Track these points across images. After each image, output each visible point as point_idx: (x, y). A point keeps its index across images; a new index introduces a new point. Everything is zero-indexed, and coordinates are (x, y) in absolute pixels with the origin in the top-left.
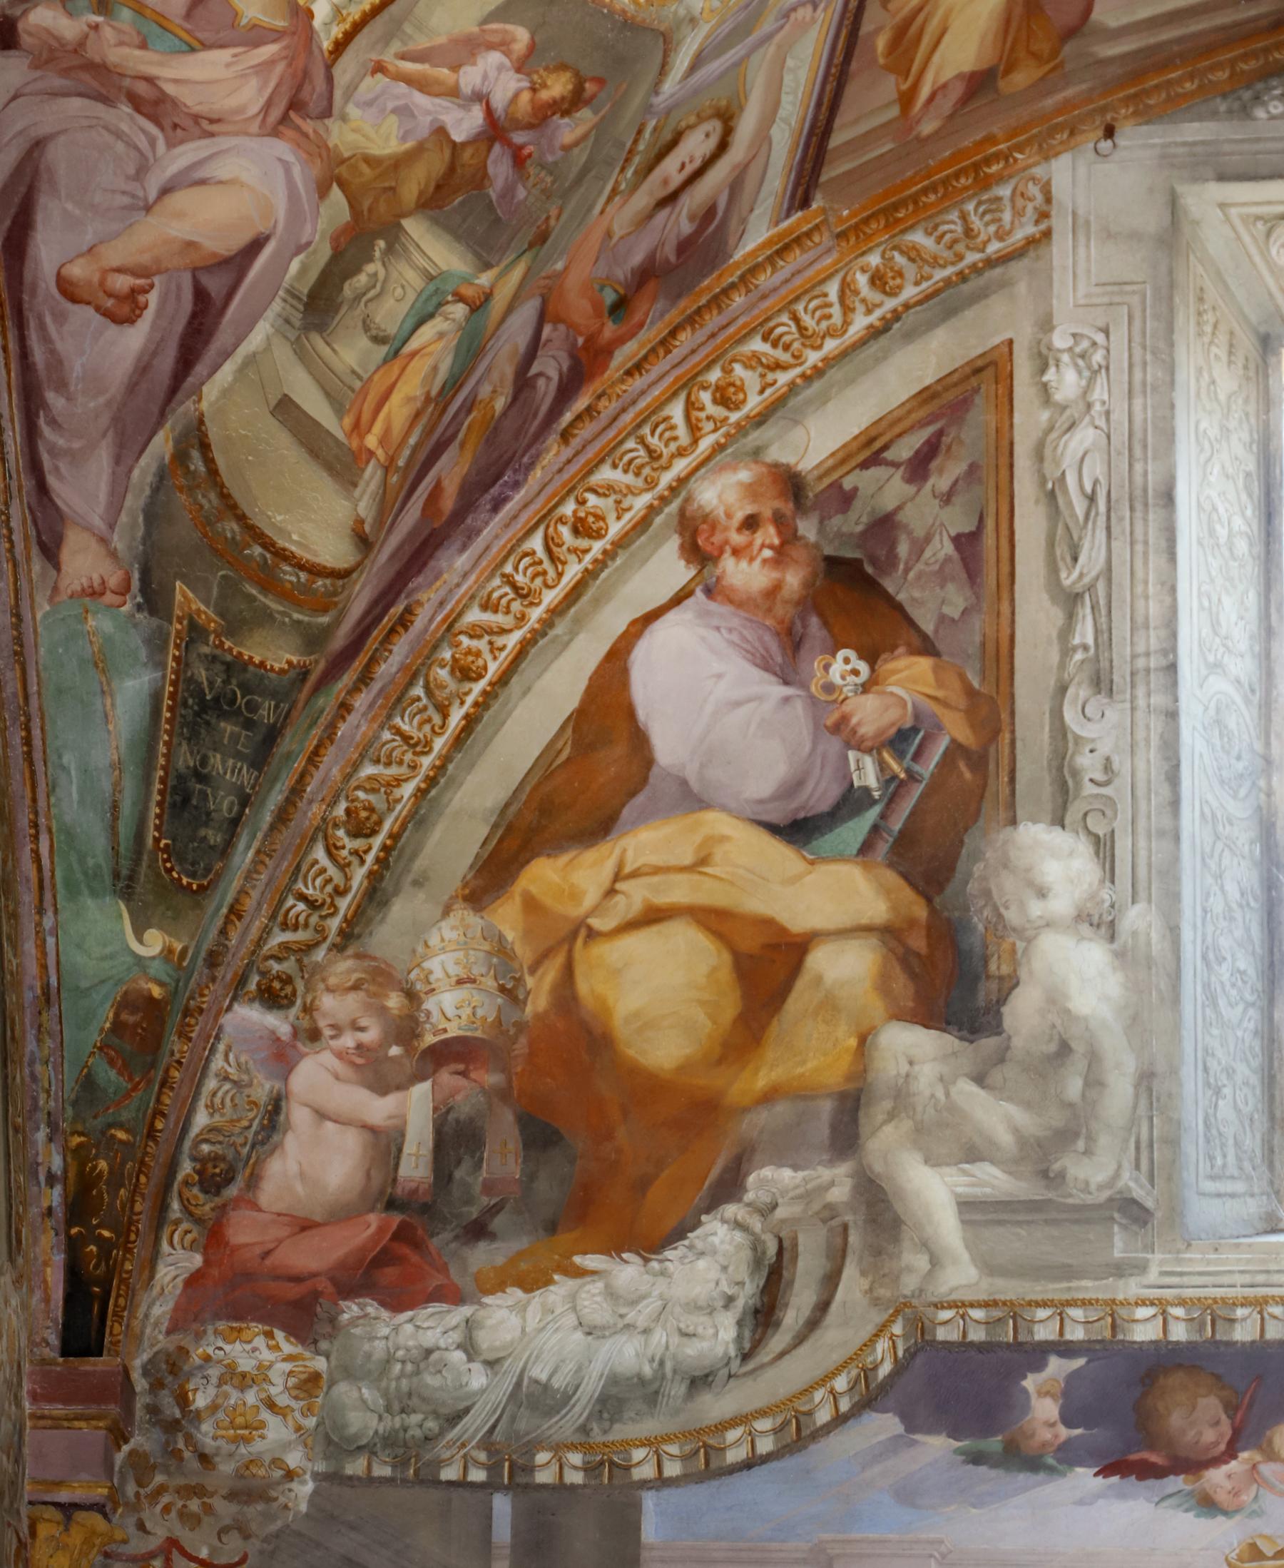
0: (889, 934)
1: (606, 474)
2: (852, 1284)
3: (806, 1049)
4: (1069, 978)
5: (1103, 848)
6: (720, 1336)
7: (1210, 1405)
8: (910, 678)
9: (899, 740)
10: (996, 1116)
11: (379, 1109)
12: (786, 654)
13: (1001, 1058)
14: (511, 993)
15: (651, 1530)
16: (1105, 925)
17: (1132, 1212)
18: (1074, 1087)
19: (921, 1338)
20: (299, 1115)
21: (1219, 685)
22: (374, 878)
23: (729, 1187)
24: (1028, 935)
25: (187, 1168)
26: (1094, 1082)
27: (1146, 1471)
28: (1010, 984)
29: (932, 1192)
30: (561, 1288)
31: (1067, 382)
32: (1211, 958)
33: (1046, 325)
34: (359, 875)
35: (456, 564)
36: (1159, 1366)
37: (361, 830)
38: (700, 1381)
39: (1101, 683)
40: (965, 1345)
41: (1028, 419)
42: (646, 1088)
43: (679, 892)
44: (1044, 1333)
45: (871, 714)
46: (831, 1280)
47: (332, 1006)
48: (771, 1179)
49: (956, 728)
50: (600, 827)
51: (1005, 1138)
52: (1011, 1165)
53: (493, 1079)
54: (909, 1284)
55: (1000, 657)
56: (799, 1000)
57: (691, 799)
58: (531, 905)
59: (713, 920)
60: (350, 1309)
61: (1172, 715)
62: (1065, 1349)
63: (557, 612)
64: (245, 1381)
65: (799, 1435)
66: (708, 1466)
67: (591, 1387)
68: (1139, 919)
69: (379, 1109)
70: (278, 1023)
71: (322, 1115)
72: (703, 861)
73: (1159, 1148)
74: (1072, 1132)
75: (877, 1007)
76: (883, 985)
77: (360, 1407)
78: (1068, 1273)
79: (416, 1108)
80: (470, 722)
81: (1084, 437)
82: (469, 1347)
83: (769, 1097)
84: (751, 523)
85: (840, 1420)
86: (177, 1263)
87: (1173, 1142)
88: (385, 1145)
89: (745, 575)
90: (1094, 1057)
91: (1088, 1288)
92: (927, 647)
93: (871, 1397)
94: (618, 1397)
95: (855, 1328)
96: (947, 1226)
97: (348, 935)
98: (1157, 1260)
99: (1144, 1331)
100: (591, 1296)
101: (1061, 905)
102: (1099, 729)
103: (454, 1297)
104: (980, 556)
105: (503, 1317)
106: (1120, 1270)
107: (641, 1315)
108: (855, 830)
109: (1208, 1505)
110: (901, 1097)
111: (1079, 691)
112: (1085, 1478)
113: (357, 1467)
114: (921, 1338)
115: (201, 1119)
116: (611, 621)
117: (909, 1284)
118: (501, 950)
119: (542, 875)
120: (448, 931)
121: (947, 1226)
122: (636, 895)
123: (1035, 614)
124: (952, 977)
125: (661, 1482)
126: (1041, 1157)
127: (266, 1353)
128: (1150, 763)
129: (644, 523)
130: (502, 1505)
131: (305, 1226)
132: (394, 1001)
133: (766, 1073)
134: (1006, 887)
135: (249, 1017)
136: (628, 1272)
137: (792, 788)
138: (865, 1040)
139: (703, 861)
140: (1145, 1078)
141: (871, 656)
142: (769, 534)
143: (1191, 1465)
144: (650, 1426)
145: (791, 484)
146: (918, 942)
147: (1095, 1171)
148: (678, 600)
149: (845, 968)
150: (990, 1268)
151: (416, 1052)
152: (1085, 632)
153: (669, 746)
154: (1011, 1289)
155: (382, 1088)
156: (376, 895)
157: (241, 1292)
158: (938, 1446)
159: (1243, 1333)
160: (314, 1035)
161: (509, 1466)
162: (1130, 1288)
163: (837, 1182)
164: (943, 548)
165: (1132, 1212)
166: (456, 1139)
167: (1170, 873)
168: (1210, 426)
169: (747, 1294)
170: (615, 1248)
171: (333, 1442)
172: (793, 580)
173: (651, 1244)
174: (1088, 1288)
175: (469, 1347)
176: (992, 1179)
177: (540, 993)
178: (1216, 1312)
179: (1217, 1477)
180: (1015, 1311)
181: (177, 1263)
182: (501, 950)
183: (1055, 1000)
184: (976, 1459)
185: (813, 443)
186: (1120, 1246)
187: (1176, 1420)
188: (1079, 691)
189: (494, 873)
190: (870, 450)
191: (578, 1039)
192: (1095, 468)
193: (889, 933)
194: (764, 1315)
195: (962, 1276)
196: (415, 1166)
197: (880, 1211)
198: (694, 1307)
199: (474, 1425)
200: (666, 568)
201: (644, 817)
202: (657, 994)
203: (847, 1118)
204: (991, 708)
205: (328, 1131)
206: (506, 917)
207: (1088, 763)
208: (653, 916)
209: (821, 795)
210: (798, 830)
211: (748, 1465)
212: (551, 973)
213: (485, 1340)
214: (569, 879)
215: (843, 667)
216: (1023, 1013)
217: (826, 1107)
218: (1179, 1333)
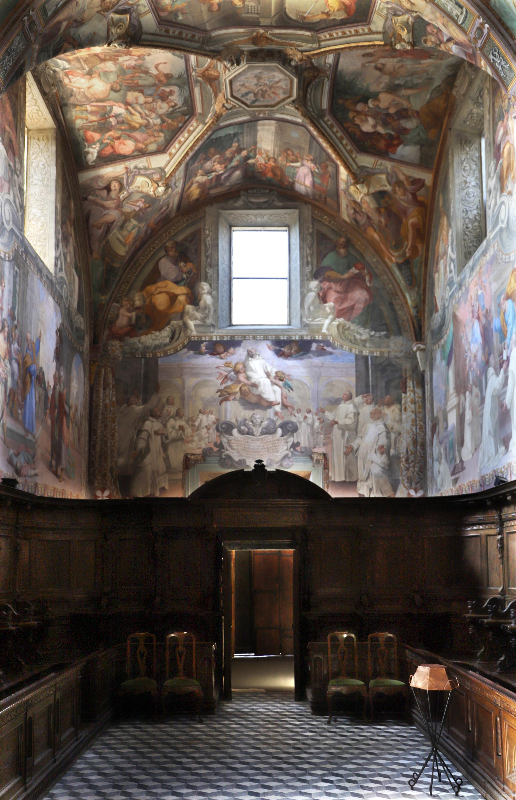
0: (187, 295)
1: (156, 242)
2: (182, 334)
3: (177, 307)
4: (207, 299)
5: (210, 285)
6: (168, 340)
7: (222, 347)
8: (190, 265)
9: (188, 272)
10: (198, 315)
11: (129, 315)
12: (176, 262)
13: (199, 308)
14: (145, 301)
15: (159, 362)
16: (210, 293)
17: (213, 326)
18: (207, 312)
19: (190, 341)
20: (120, 316)
21: (224, 266)
22: (130, 288)
23: (169, 323)
24: (202, 294)
25: (108, 322)
26: (209, 311)
27: (215, 355)
28: (200, 300)
29: (191, 324)
30: (149, 336)
31: (207, 232)
32: (222, 296)
33: (205, 226)
34: (127, 288)
35: (140, 253)
36: (216, 342)
37: (128, 282)
38: (165, 345)
39: (210, 266)
40: (195, 341)
41: (203, 236)
42: (160, 312)
43: (163, 290)
44: (203, 339)
45: (185, 269)
46: (180, 334)
47: (124, 303)
48: (174, 322)
49: (194, 271)
50: (154, 282)
51: (199, 317)
52: (200, 320)
53: (142, 311)
54: (189, 334)
55: (199, 263)
56: (177, 302)
57: (165, 279)
58: (147, 291)
59: (167, 293)
60: (126, 338)
61: (218, 270)
62: (206, 341)
63: (151, 257)
64: (114, 346)
65: (176, 351)
66: (166, 355)
67: (153, 346)
68: (214, 293)
69: (129, 315)
70: (118, 305)
71: (123, 315)
72: (166, 286)
73: (217, 318)
74: (207, 317)
75: (185, 303)
76: (186, 300)
77: (127, 349)
78: (206, 333)
79: (134, 314)
80: (141, 270)
81: (209, 238)
82: (139, 342)
83: (173, 313)
84: (172, 248)
85: (181, 350)
86: (107, 332)
87: (218, 318)
88: (130, 319)
89: (172, 253)
90: (209, 308)
91: (208, 334)
92: (191, 262)
93: (184, 347)
94: (157, 347)
95: (183, 340)
96: (193, 327)
97: (126, 295)
98: (216, 331)
99: (214, 339)
100: (153, 336)
101: (206, 291)
102: (210, 271)
103: (138, 336)
104: (197, 252)
105: (143, 338)
106: (212, 332)
107: (159, 338)
108: (183, 283)
109: (221, 358)
110: (188, 313)
111: (208, 267)
112: (208, 356)
113: (126, 356)
114: (190, 341)
115: (109, 316)
116: (157, 258)
117: (189, 334)
118: (143, 296)
119: (148, 288)
120: (137, 294)
121: (193, 327)
122: (159, 290)
123: (203, 258)
124: (194, 299)
125: (161, 357)
126: (203, 320)
127: (117, 343)
128: (216, 275)
129: (161, 247)
130: (143, 360)
131: (121, 328)
132: (131, 302)
133: (173, 310)
134: (200, 289)
135: (115, 304)
136: (157, 333)
137: (176, 278)
138: (184, 307)
139: (166, 286)
140: (215, 311)
141: (185, 263)
142: (174, 249)
143: (219, 354)
144: (159, 351)
145: (177, 243)
146: (190, 295)
147: (209, 321)
148: (164, 256)
149: (182, 298)
150: (197, 332)
151: (133, 308)
152: (209, 261)
153: (163, 273)
154: (200, 335)
155: (130, 312)
156: (129, 290)
157: (114, 336)
158: (192, 352)
159: (225, 339)
160: (122, 306)
161: (144, 355)
162: (213, 334)
163: (181, 322)
164: (194, 251)
165: (213, 326)
166: (138, 318)
167: (218, 288)
168: (223, 237)
169: (170, 335)
170: (156, 330)
171: (124, 353)
172: (177, 254)
173: (160, 330)
174: (208, 334)
175: (139, 342)
176: (198, 322)
177: (148, 302)
178: (222, 337)
179: (222, 355)
180: (201, 337)
181: (107, 332)
182: (143, 296)
183: (205, 302)
184: (196, 354)
185: (180, 238)
186: (212, 330)
187: (218, 349)
188: (208, 267)
189: (143, 288)
190: (185, 239)
191: (152, 307)
192: (210, 242)
193: (187, 295)
194: (172, 338)
195: (194, 333)
196: (133, 321)
197: (185, 326)
198: (164, 337)
199: (140, 350)
200: (163, 253)
201: (160, 281)
202: (161, 301)
203: (182, 315)
204: (198, 269)
205: (124, 317)
206: (144, 293)
207: (209, 275)
208: (160, 293)
209: (180, 279)
210: (177, 283)
211: (171, 354)
212: (149, 299)
213: (141, 341)
214: (152, 288)
215: (182, 264)
216: (202, 303)
217: (179, 314)
218: (218, 339)
